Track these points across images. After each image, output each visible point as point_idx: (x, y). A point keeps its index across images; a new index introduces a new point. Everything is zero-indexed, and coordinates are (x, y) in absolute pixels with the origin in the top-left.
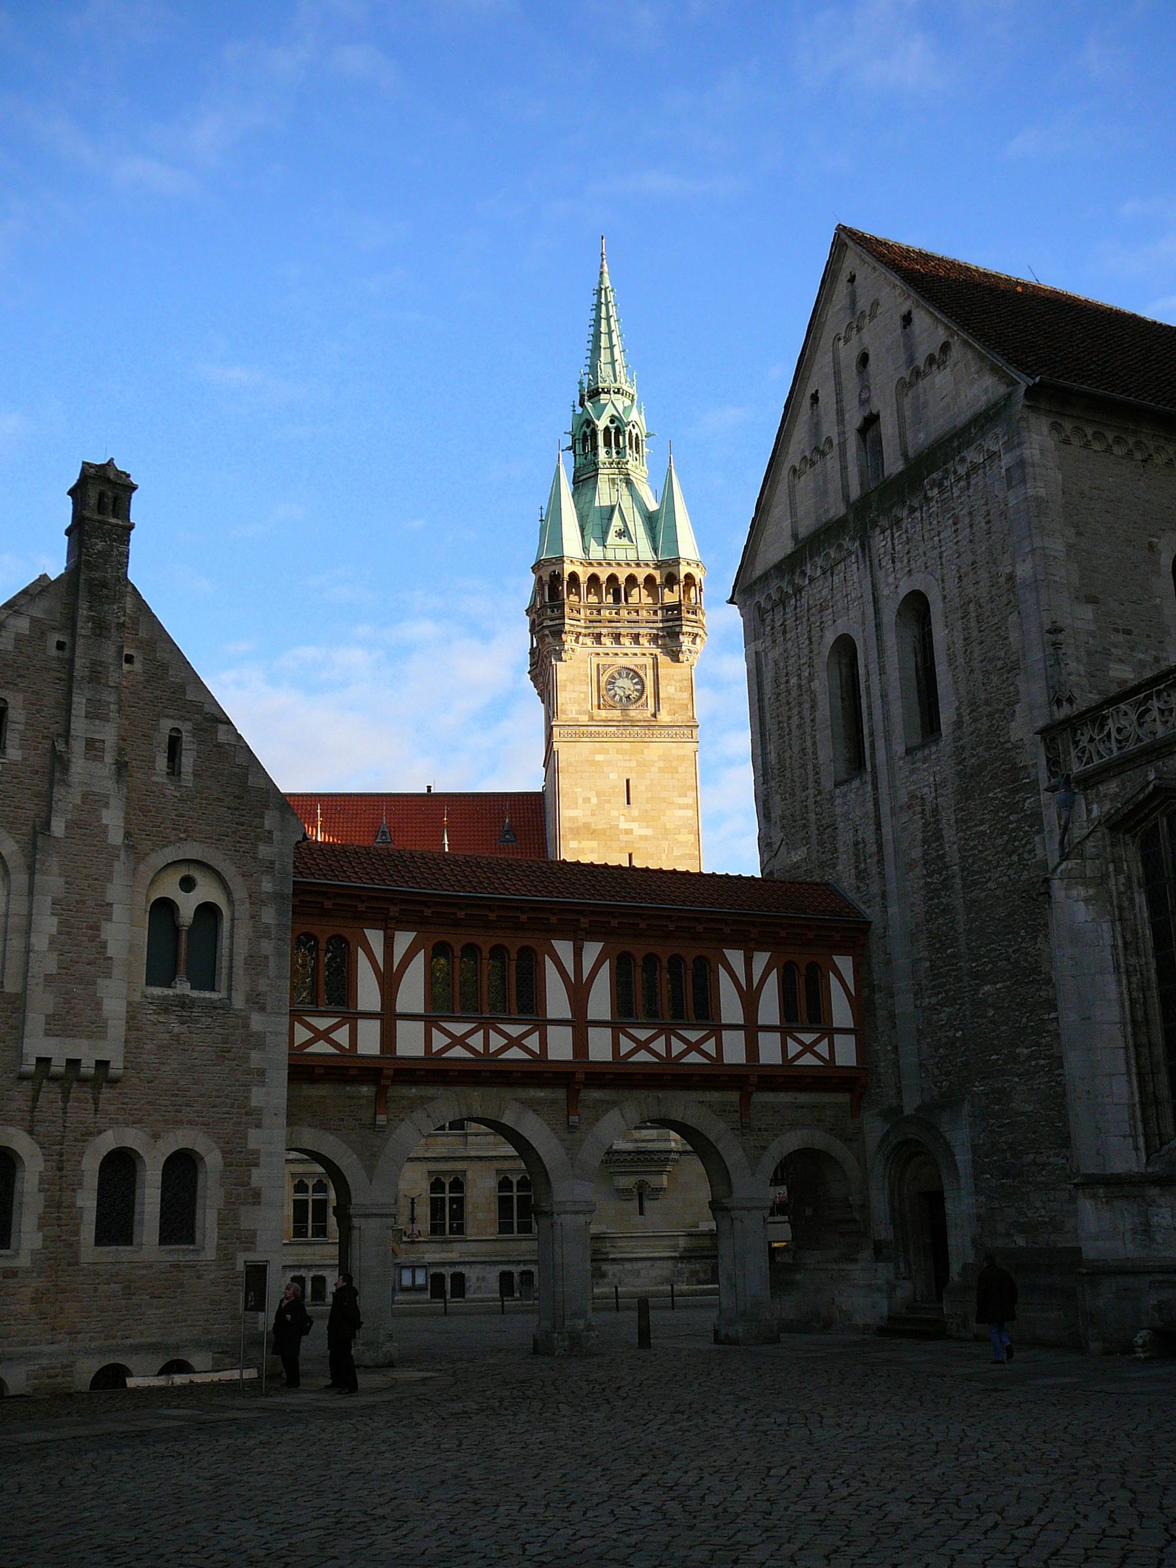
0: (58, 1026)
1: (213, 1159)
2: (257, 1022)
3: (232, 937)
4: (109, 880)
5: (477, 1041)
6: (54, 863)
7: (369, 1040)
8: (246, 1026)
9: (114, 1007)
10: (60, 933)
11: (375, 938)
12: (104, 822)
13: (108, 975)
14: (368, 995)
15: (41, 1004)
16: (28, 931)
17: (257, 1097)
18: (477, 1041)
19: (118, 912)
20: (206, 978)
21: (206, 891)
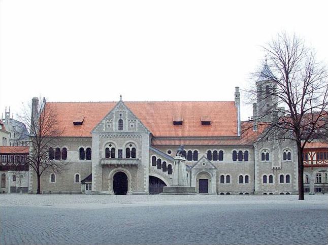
0: (274, 165)
1: (290, 176)
2: (294, 163)
5: (322, 162)
7: (310, 163)
11: (310, 153)
14: (310, 159)
17: (295, 170)
18: (322, 162)
19: (280, 154)
20: (289, 159)
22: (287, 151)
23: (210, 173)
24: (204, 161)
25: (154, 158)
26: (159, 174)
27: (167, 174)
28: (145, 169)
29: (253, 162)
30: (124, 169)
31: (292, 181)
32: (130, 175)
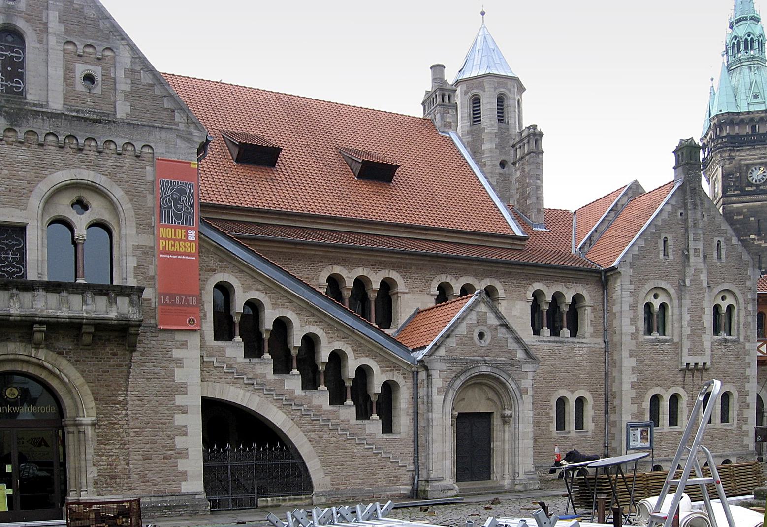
3: (739, 316)
4: (703, 299)
6: (687, 296)
8: (744, 348)
9: (707, 345)
10: (690, 320)
12: (701, 279)
13: (705, 333)
15: (687, 345)
16: (681, 319)
21: (729, 301)
22: (723, 298)
23: (511, 385)
24: (482, 320)
25: (224, 289)
26: (256, 385)
27: (299, 391)
28: (176, 353)
29: (600, 340)
30: (42, 354)
31: (738, 415)
32: (86, 389)
